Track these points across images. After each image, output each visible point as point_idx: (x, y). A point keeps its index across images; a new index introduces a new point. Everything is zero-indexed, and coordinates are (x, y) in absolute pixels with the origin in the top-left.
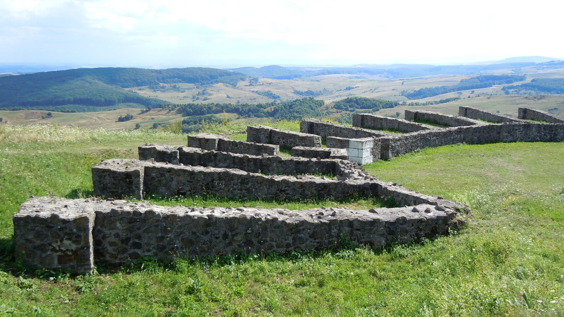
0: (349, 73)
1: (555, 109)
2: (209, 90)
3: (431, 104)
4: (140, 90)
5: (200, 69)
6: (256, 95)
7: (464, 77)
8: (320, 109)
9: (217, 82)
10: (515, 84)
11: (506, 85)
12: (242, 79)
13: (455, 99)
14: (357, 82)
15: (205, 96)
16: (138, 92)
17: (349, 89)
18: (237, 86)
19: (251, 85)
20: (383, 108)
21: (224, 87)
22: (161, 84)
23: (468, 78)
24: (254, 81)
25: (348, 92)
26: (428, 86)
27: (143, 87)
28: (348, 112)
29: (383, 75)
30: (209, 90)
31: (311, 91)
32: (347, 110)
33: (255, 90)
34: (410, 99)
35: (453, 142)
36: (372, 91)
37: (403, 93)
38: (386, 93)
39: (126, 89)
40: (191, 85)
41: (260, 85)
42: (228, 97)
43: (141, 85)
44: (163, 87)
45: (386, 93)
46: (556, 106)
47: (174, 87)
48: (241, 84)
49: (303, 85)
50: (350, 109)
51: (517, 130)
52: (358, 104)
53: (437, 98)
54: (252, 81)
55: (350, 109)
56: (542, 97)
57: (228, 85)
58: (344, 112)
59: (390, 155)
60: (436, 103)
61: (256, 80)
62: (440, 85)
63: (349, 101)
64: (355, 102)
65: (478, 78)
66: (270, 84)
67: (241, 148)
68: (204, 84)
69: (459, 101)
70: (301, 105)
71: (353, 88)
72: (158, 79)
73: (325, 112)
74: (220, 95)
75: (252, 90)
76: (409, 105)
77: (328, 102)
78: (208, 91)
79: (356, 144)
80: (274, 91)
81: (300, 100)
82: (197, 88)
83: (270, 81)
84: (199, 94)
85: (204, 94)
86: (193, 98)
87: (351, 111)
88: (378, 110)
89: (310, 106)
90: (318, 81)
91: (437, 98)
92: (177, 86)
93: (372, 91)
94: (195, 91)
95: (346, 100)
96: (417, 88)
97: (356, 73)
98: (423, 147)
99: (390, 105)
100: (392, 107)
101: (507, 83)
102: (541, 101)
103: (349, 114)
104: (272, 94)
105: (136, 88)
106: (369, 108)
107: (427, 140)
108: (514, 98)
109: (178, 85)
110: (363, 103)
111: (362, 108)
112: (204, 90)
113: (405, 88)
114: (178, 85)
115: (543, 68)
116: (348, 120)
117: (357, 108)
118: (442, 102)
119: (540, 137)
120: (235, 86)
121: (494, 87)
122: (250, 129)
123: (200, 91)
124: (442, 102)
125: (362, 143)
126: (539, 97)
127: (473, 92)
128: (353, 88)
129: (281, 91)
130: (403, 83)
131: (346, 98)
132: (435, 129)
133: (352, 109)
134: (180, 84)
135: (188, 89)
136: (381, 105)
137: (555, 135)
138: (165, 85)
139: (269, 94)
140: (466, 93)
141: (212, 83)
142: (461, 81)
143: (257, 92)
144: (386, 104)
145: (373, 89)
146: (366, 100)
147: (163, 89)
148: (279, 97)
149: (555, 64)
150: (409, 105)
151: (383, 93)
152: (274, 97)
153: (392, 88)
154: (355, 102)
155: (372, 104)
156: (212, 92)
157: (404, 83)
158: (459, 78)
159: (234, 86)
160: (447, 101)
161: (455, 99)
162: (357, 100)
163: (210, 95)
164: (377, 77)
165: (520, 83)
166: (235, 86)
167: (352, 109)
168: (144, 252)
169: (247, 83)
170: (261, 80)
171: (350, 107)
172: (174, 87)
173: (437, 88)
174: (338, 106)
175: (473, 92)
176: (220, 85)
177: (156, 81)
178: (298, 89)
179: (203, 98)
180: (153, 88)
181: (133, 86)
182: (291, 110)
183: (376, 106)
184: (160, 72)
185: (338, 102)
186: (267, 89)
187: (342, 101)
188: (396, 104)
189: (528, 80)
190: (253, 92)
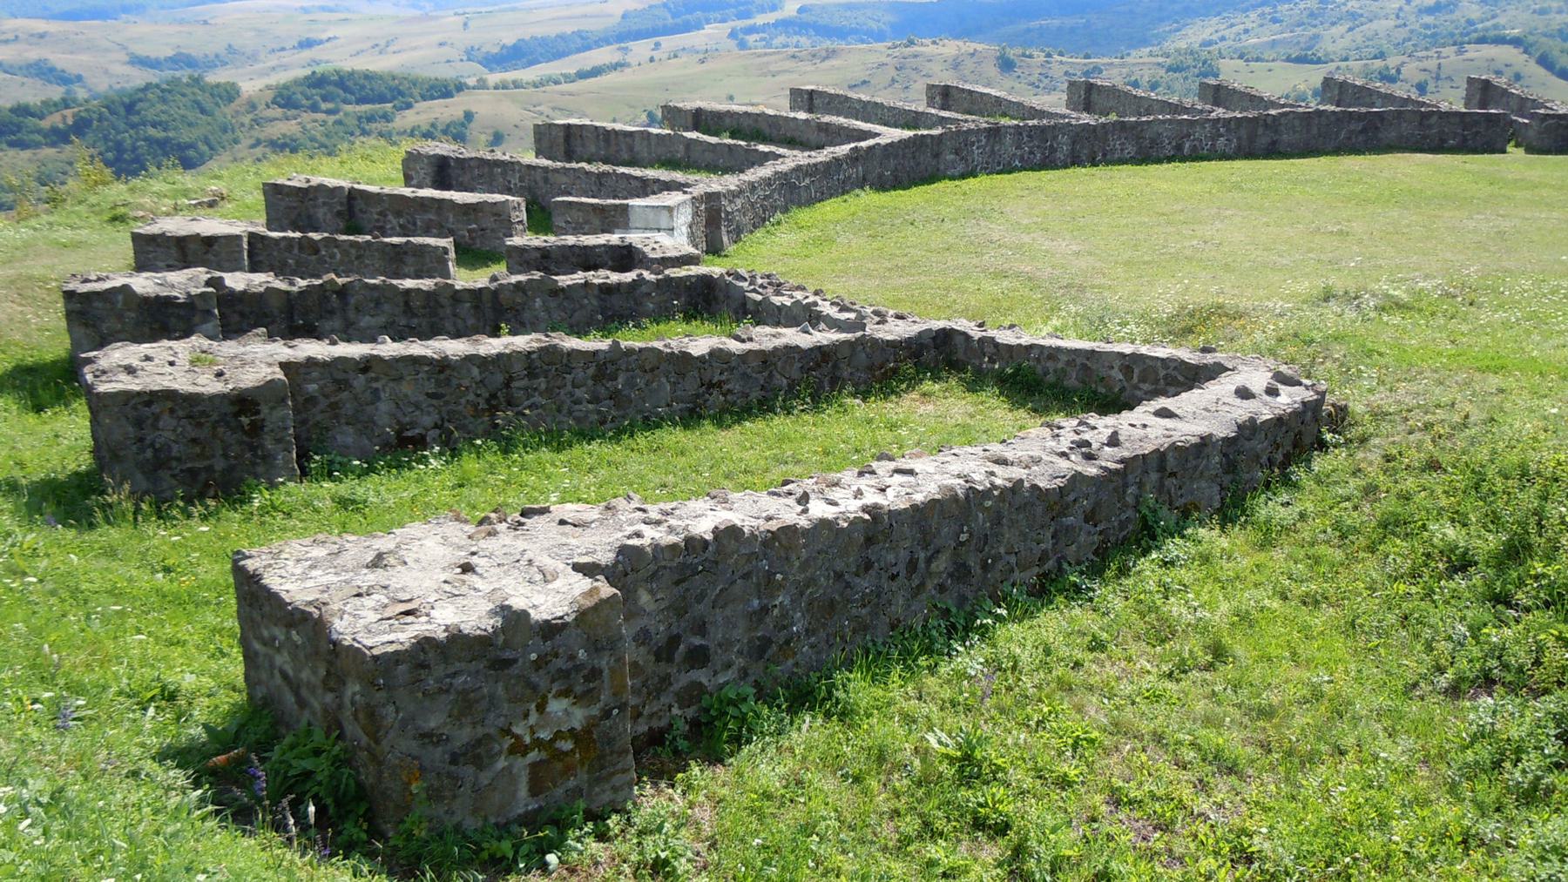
1: (864, 82)
3: (557, 83)
8: (228, 110)
10: (760, 20)
11: (740, 24)
13: (615, 67)
17: (307, 44)
20: (424, 98)
25: (307, 54)
26: (539, 31)
28: (320, 116)
31: (188, 56)
32: (314, 108)
35: (843, 188)
36: (380, 48)
37: (470, 54)
46: (862, 76)
50: (324, 106)
51: (973, 144)
52: (346, 89)
53: (569, 65)
56: (831, 54)
58: (307, 117)
59: (725, 239)
60: (569, 79)
63: (317, 82)
64: (336, 84)
66: (42, 36)
67: (332, 256)
69: (628, 70)
70: (164, 101)
71: (321, 42)
73: (247, 119)
76: (496, 88)
77: (251, 86)
79: (651, 215)
80: (60, 60)
81: (157, 86)
83: (40, 26)
87: (329, 112)
88: (409, 106)
89: (197, 102)
90: (205, 22)
91: (569, 65)
93: (380, 48)
95: (307, 78)
96: (509, 39)
98: (785, 210)
99: (443, 90)
100: (447, 94)
101: (740, 16)
102: (828, 63)
103: (324, 123)
104: (52, 70)
106: (382, 99)
107: (793, 187)
108: (765, 59)
110: (363, 87)
113: (472, 38)
116: (323, 139)
117: (346, 102)
118: (582, 75)
119: (1022, 159)
121: (709, 29)
122: (274, 192)
124: (582, 75)
125: (670, 209)
126: (824, 54)
127: (657, 45)
128: (321, 42)
129: (84, 58)
130: (465, 24)
131: (308, 72)
132: (793, 159)
133: (330, 106)
136: (416, 92)
137: (1053, 150)
139: (43, 71)
140: (640, 49)
142: (624, 17)
144: (432, 87)
145: (382, 43)
146: (368, 76)
148: (79, 78)
150: (496, 88)
152: (63, 79)
154: (336, 84)
155: (391, 89)
160: (596, 72)
161: (615, 67)
162: (341, 78)
167: (330, 106)
168: (715, 673)
171: (325, 99)
173: (562, 37)
174: (285, 99)
175: (657, 45)
178: (141, 50)
182: (135, 119)
183: (401, 93)
185: (286, 87)
186: (33, 54)
187: (296, 82)
188: (460, 87)
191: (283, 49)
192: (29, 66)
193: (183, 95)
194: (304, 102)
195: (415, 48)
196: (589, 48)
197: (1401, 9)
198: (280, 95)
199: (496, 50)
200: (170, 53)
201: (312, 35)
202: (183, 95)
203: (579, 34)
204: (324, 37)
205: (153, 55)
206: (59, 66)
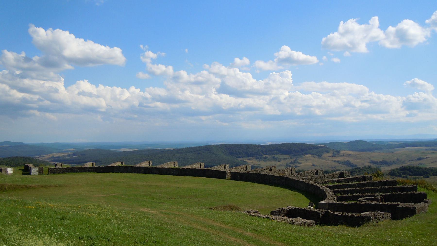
2: (299, 160)
4: (249, 159)
5: (294, 144)
6: (337, 164)
9: (306, 154)
12: (327, 152)
14: (428, 153)
16: (247, 161)
17: (420, 159)
18: (322, 157)
19: (333, 156)
20: (434, 175)
21: (311, 158)
22: (264, 156)
24: (336, 153)
25: (419, 162)
27: (252, 158)
30: (299, 160)
33: (337, 160)
39: (240, 159)
40: (287, 156)
41: (341, 156)
42: (313, 165)
43: (250, 156)
44: (265, 158)
47: (274, 157)
48: (325, 155)
49: (378, 156)
50: (403, 176)
54: (335, 153)
55: (403, 176)
57: (315, 156)
61: (338, 152)
63: (403, 169)
64: (408, 170)
66: (350, 155)
68: (296, 155)
70: (360, 171)
72: (262, 152)
74: (308, 164)
75: (334, 160)
77: (385, 169)
78: (298, 160)
80: (352, 161)
81: (360, 168)
82: (291, 158)
83: (350, 152)
84: (291, 163)
85: (295, 163)
86: (287, 165)
88: (428, 177)
90: (393, 153)
92: (276, 157)
94: (289, 161)
95: (400, 168)
97: (433, 146)
104: (350, 163)
105: (246, 158)
109: (276, 156)
111: (414, 175)
112: (295, 160)
114: (276, 156)
117: (410, 175)
120: (320, 157)
123: (292, 160)
128: (424, 159)
133: (404, 175)
134: (278, 156)
135: (284, 159)
138: (267, 156)
139: (348, 163)
141: (302, 155)
143: (338, 161)
147: (265, 159)
152: (352, 165)
154: (408, 170)
156: (301, 162)
159: (320, 157)
162: (410, 168)
163: (300, 163)
166: (320, 157)
167: (404, 175)
169: (330, 154)
170: (342, 152)
171: (403, 174)
172: (274, 157)
174: (392, 173)
176: (309, 156)
177: (261, 153)
178: (374, 159)
180: (258, 158)
181: (245, 157)
183: (427, 173)
184: (264, 146)
185: (393, 170)
186: (346, 159)
187: (397, 169)
190: (335, 161)
191: (412, 160)
193: (365, 171)
194: (397, 174)
198: (391, 172)
200: (381, 160)
201: (421, 157)
202: (365, 171)
204: (425, 157)
205: (376, 161)
206: (352, 163)
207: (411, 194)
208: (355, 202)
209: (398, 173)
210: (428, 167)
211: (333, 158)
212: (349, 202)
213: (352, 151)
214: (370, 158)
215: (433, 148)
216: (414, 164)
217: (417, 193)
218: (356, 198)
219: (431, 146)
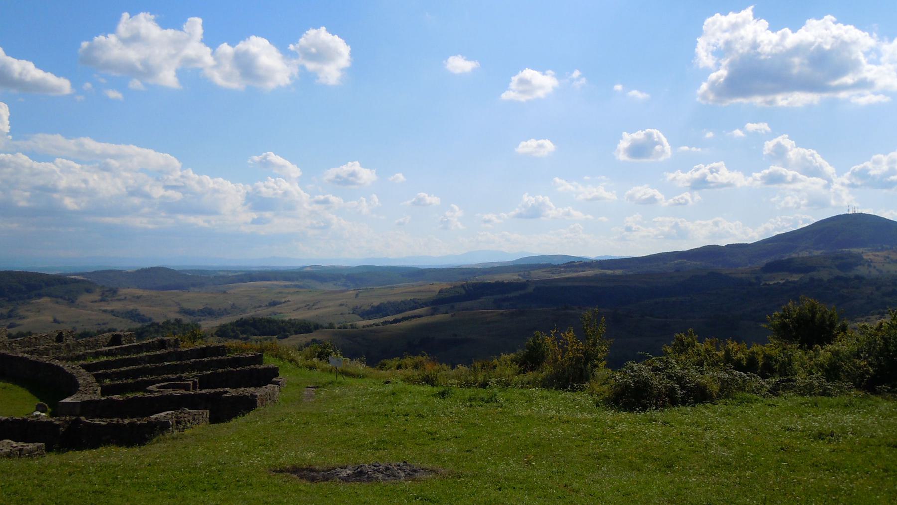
0: (286, 279)
2: (21, 311)
6: (108, 317)
7: (445, 285)
9: (40, 296)
10: (511, 295)
12: (88, 291)
14: (288, 293)
15: (13, 320)
17: (273, 304)
19: (101, 301)
20: (296, 333)
23: (449, 287)
24: (110, 293)
25: (271, 309)
26: (392, 299)
29: (339, 283)
30: (21, 311)
33: (109, 308)
34: (364, 319)
36: (309, 307)
37: (355, 310)
38: (328, 309)
41: (119, 300)
42: (55, 321)
45: (328, 309)
48: (84, 298)
49: (195, 299)
50: (241, 336)
55: (241, 336)
57: (60, 300)
61: (114, 291)
62: (409, 298)
63: (242, 323)
65: (463, 286)
66: (138, 297)
71: (280, 303)
77: (208, 324)
80: (143, 309)
81: (158, 324)
83: (139, 292)
85: (10, 316)
88: (286, 337)
90: (225, 292)
93: (309, 307)
96: (376, 302)
104: (138, 314)
112: (12, 310)
115: (560, 272)
117: (255, 334)
120: (73, 302)
128: (280, 303)
130: (357, 295)
131: (238, 317)
133: (245, 336)
139: (133, 315)
141: (30, 298)
142: (440, 292)
143: (112, 311)
145: (311, 304)
149: (576, 266)
151: (325, 310)
152: (142, 319)
153: (339, 302)
157: (360, 295)
158: (437, 287)
159: (72, 301)
163: (22, 318)
164: (330, 287)
165: (516, 294)
166: (73, 302)
167: (245, 336)
169: (96, 296)
170: (123, 291)
171: (243, 332)
173: (404, 302)
174: (222, 332)
178: (186, 305)
179: (8, 323)
183: (284, 330)
185: (225, 326)
186: (131, 307)
187: (231, 323)
189: (530, 289)
190: (105, 311)
191: (260, 306)
192: (128, 312)
193: (169, 329)
195: (326, 307)
196: (416, 308)
197: (872, 294)
199: (368, 308)
200: (201, 307)
201: (277, 300)
203: (413, 301)
206: (142, 313)
207: (252, 370)
208: (139, 395)
209: (233, 331)
210: (286, 319)
211: (102, 303)
212: (127, 395)
213: (145, 288)
214: (179, 304)
215: (296, 283)
216: (263, 313)
217: (261, 367)
218: (142, 386)
219: (293, 280)
